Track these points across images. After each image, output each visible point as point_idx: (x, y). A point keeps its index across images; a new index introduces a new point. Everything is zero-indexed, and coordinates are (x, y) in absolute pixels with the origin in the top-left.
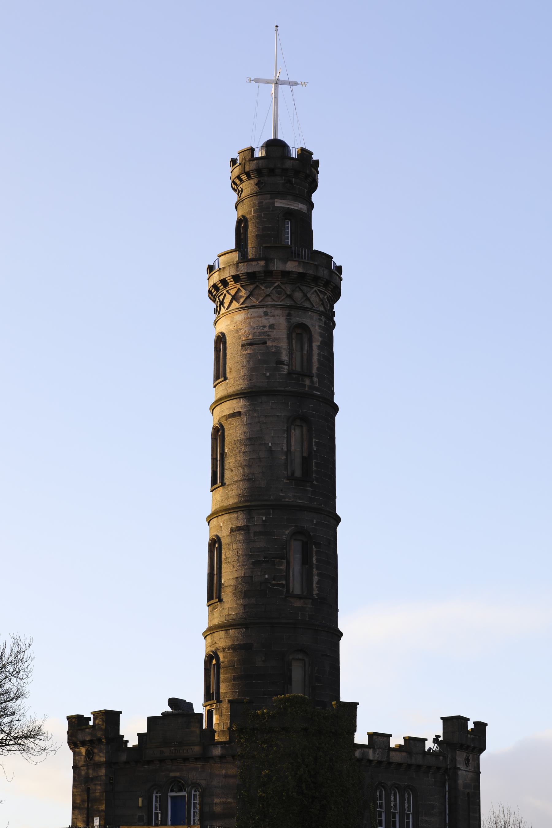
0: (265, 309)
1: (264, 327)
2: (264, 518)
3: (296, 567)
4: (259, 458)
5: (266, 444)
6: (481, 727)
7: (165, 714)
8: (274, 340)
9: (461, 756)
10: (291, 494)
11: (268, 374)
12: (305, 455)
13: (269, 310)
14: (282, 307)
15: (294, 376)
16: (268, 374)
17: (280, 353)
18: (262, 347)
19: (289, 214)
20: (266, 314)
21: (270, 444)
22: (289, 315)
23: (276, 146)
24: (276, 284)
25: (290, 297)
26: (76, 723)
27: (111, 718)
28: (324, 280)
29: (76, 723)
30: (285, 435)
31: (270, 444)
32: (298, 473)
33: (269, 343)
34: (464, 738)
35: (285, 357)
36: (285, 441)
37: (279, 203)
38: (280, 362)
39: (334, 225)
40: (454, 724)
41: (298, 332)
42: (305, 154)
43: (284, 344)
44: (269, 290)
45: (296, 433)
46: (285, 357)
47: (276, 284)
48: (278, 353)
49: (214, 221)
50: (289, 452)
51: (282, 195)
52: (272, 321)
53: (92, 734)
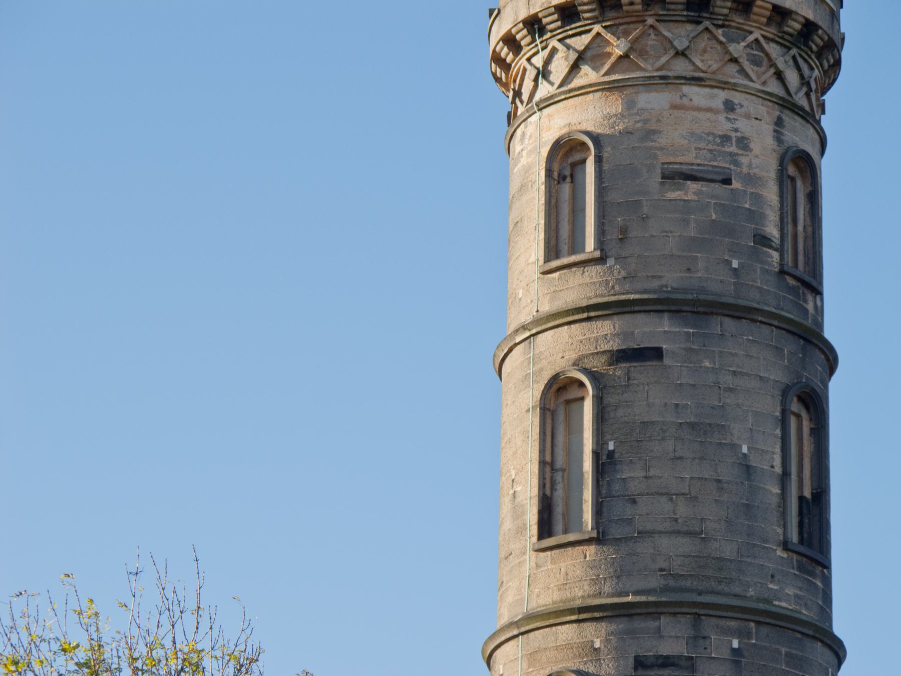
0: (722, 95)
1: (726, 138)
2: (735, 644)
4: (719, 481)
5: (735, 447)
8: (750, 179)
10: (790, 591)
11: (735, 264)
12: (807, 493)
13: (737, 98)
14: (767, 96)
15: (791, 282)
16: (735, 264)
17: (763, 216)
18: (718, 189)
20: (729, 106)
21: (745, 449)
22: (779, 122)
24: (751, 38)
25: (779, 76)
30: (778, 432)
31: (745, 449)
32: (794, 537)
33: (736, 185)
35: (772, 231)
36: (778, 450)
38: (763, 240)
43: (771, 194)
44: (737, 49)
46: (772, 231)
47: (751, 38)
48: (755, 216)
52: (744, 125)
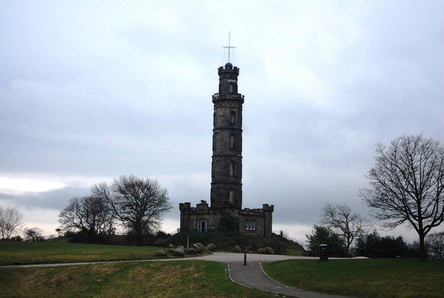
3: (231, 169)
6: (272, 206)
7: (200, 204)
9: (267, 213)
19: (231, 83)
23: (229, 66)
26: (181, 205)
27: (188, 204)
28: (240, 100)
29: (181, 205)
34: (268, 210)
37: (229, 81)
39: (244, 85)
40: (266, 206)
41: (233, 113)
42: (236, 68)
45: (232, 138)
49: (214, 86)
50: (230, 142)
51: (229, 79)
53: (185, 208)
